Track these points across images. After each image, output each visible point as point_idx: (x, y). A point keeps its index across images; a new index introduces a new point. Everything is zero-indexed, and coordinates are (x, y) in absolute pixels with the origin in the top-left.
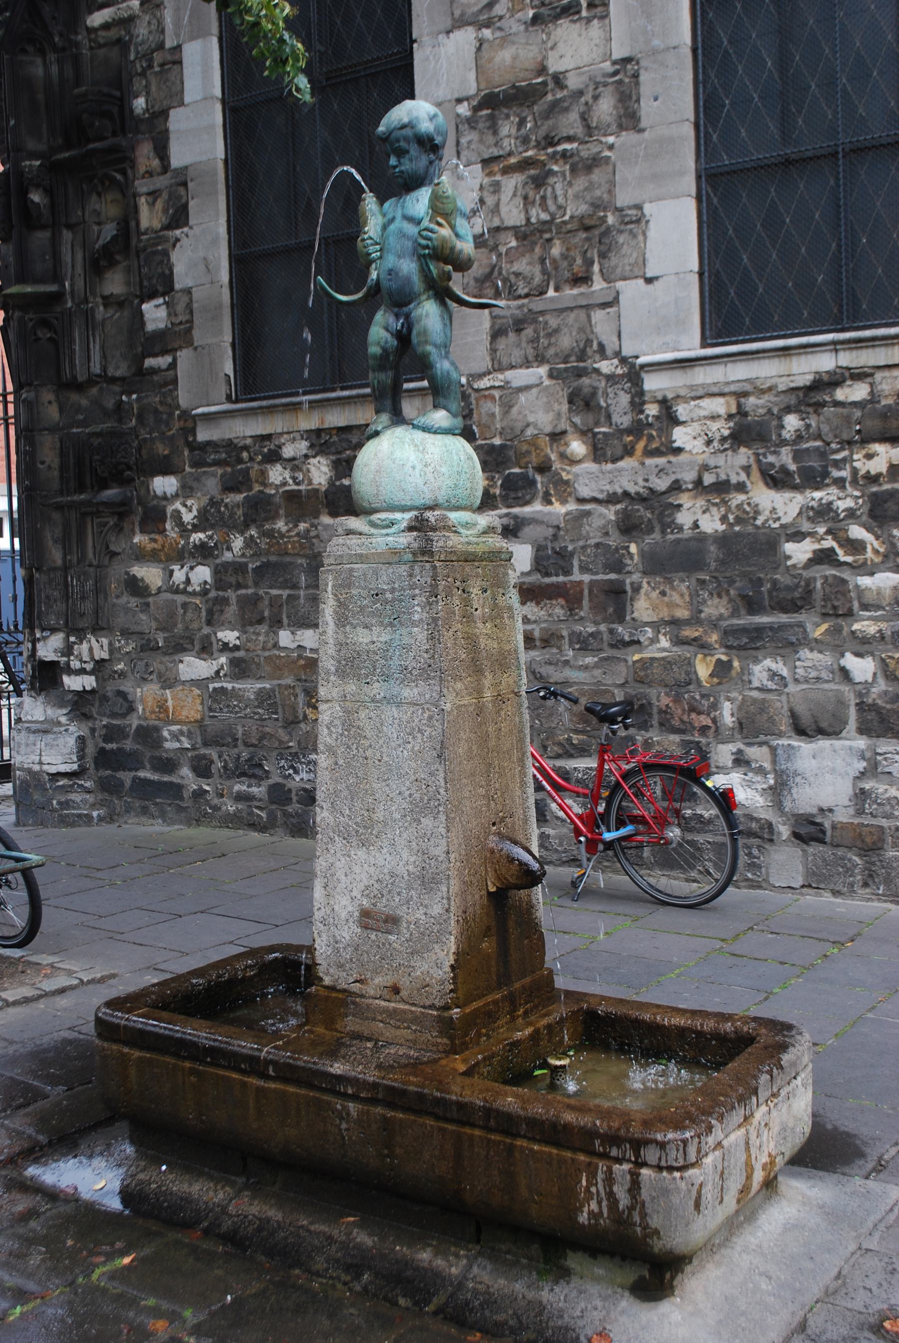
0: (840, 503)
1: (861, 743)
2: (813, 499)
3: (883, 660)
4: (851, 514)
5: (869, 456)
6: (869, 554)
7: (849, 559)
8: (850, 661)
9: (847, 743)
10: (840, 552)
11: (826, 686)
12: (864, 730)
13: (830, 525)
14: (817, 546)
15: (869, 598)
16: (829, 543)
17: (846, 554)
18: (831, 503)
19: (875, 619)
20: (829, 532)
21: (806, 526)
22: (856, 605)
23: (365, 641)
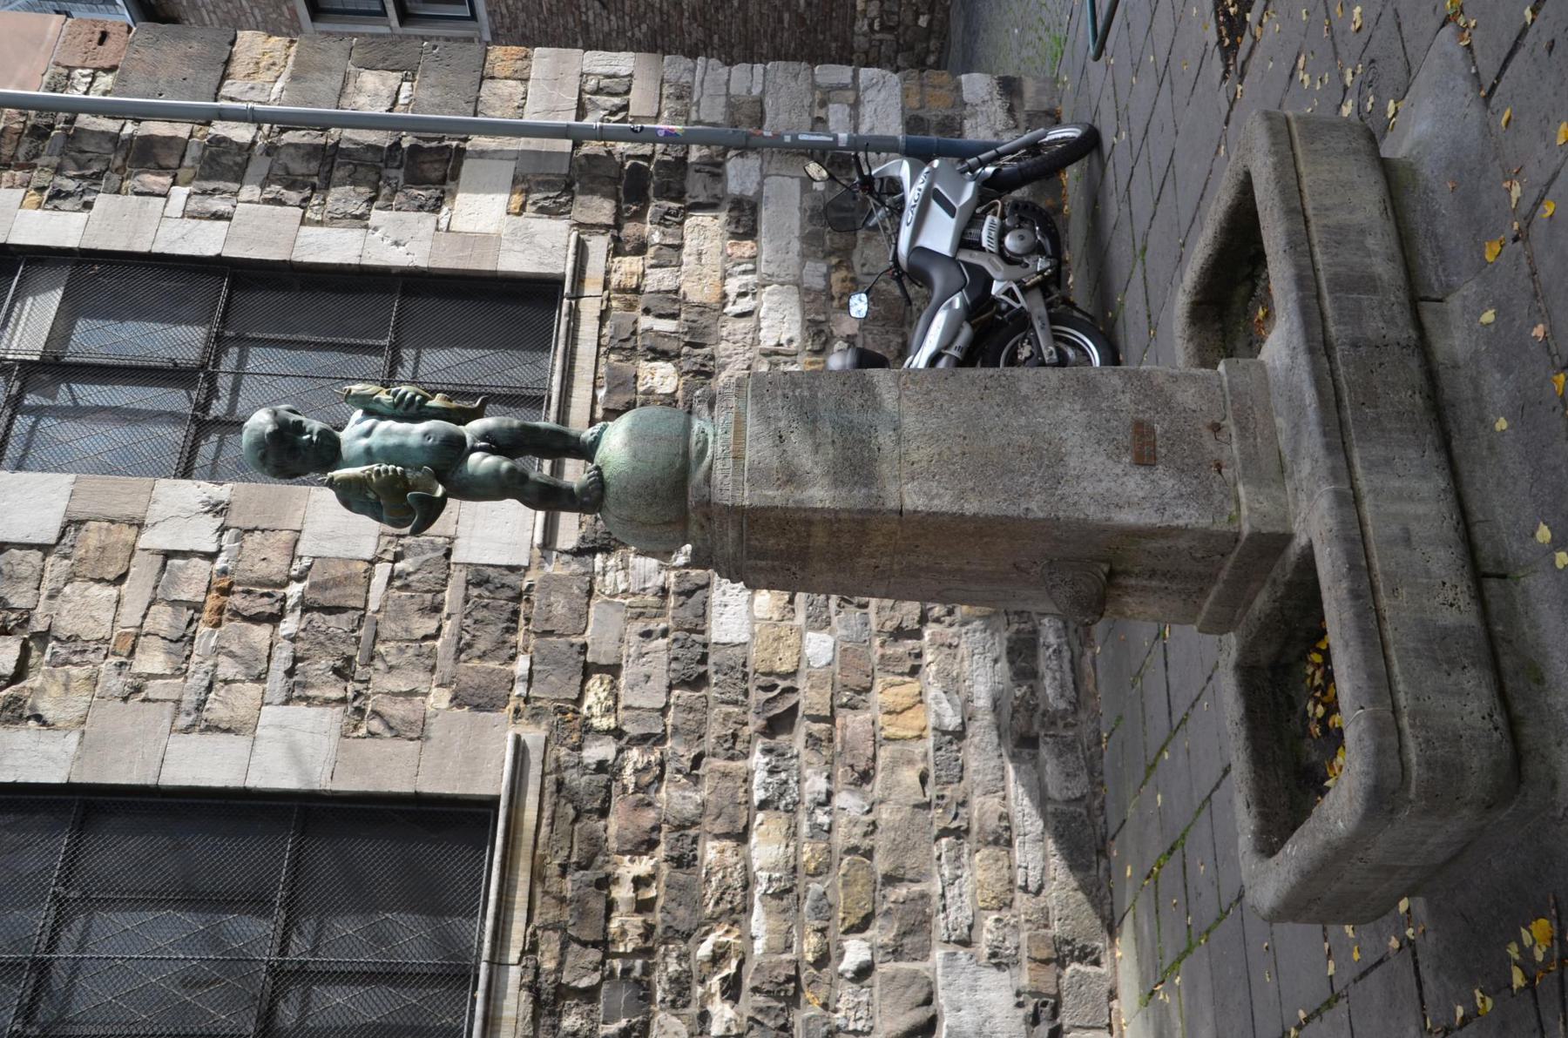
0: (670, 969)
1: (938, 954)
2: (663, 1001)
3: (846, 932)
4: (683, 957)
5: (624, 933)
6: (731, 938)
7: (734, 963)
8: (850, 963)
9: (939, 971)
10: (725, 972)
11: (876, 995)
12: (924, 953)
13: (694, 982)
14: (717, 998)
15: (779, 943)
16: (715, 983)
17: (729, 965)
18: (671, 981)
19: (802, 937)
20: (702, 982)
21: (694, 1009)
22: (787, 957)
23: (831, 451)
